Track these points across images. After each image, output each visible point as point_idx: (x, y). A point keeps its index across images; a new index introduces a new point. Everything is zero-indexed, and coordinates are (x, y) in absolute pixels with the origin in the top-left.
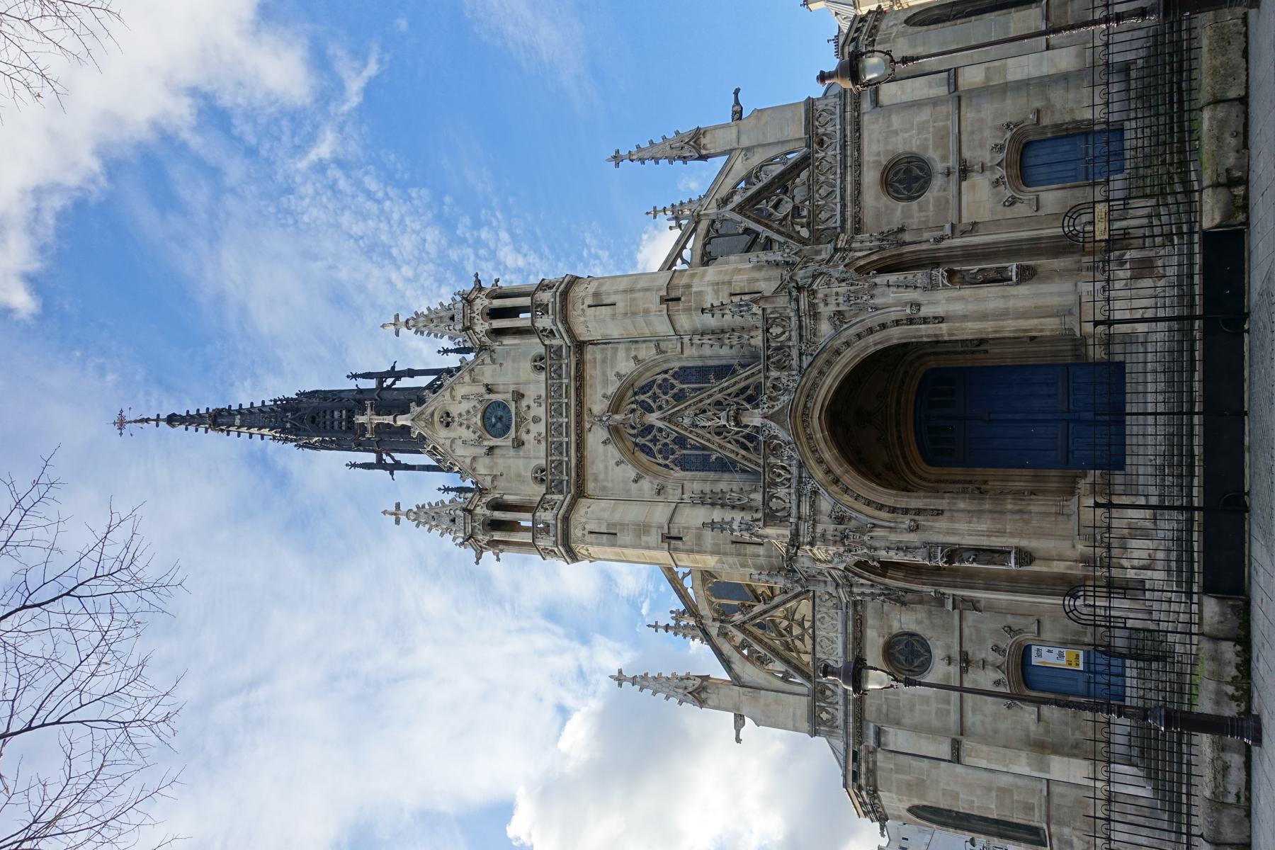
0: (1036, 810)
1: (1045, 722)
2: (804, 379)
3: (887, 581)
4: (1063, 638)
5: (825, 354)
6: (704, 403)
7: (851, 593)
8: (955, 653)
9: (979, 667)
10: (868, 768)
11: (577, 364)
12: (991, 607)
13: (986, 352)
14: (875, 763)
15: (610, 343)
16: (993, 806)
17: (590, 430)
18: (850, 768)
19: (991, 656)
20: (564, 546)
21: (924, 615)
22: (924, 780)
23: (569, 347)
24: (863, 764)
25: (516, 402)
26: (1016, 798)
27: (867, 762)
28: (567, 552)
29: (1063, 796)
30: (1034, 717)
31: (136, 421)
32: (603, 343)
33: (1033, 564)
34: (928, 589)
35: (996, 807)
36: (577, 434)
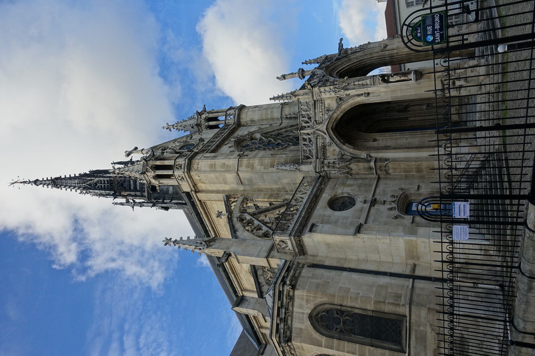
0: (403, 298)
1: (417, 223)
2: (336, 62)
3: (344, 147)
4: (431, 191)
5: (346, 59)
6: (281, 131)
7: (323, 163)
8: (370, 197)
9: (381, 203)
10: (294, 275)
11: (234, 128)
12: (394, 160)
13: (407, 118)
14: (300, 273)
15: (251, 125)
16: (372, 296)
17: (226, 144)
18: (283, 274)
19: (389, 199)
20: (189, 159)
21: (356, 187)
22: (329, 282)
23: (235, 123)
24: (292, 272)
25: (200, 142)
26: (389, 290)
27: (295, 271)
28: (188, 163)
29: (422, 289)
30: (411, 221)
31: (21, 182)
32: (249, 126)
33: (422, 79)
34: (363, 155)
35: (375, 296)
36: (220, 143)
